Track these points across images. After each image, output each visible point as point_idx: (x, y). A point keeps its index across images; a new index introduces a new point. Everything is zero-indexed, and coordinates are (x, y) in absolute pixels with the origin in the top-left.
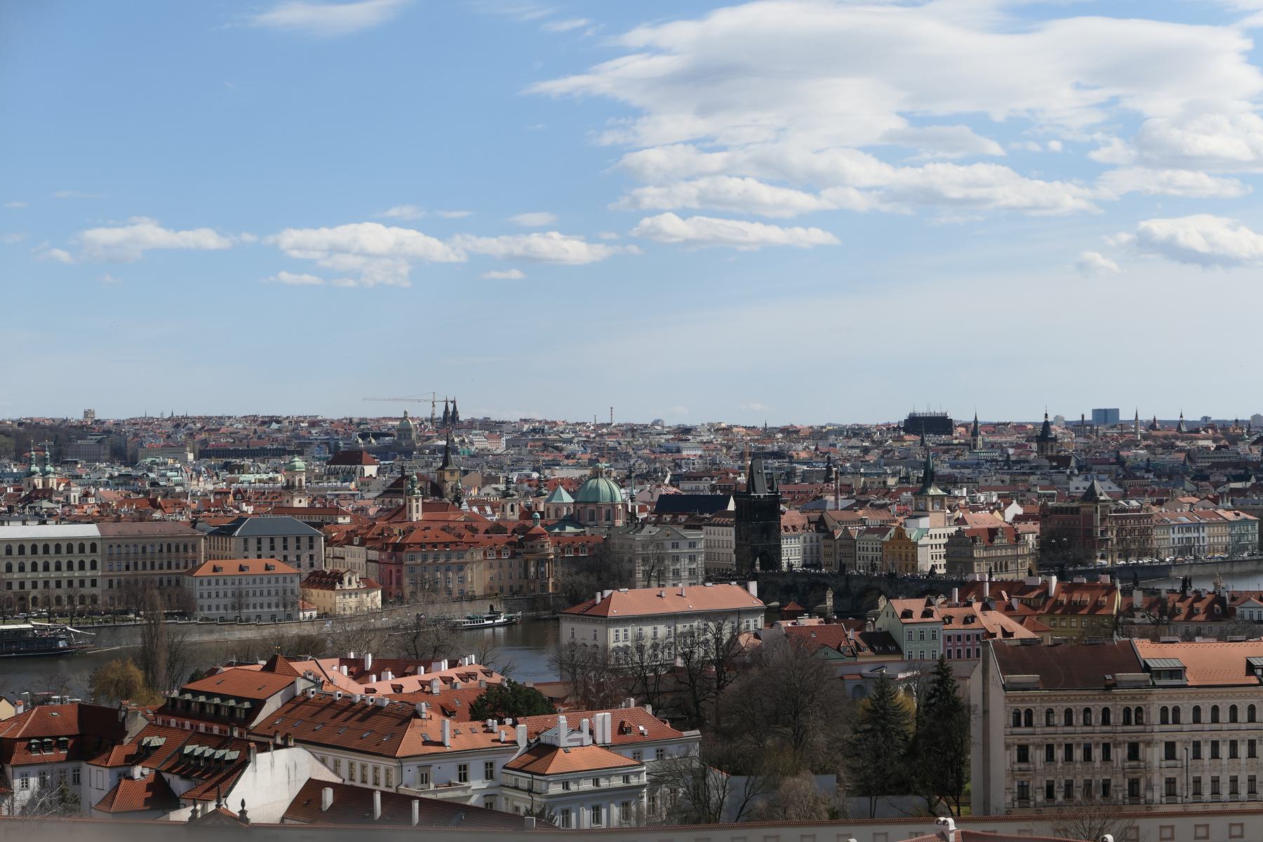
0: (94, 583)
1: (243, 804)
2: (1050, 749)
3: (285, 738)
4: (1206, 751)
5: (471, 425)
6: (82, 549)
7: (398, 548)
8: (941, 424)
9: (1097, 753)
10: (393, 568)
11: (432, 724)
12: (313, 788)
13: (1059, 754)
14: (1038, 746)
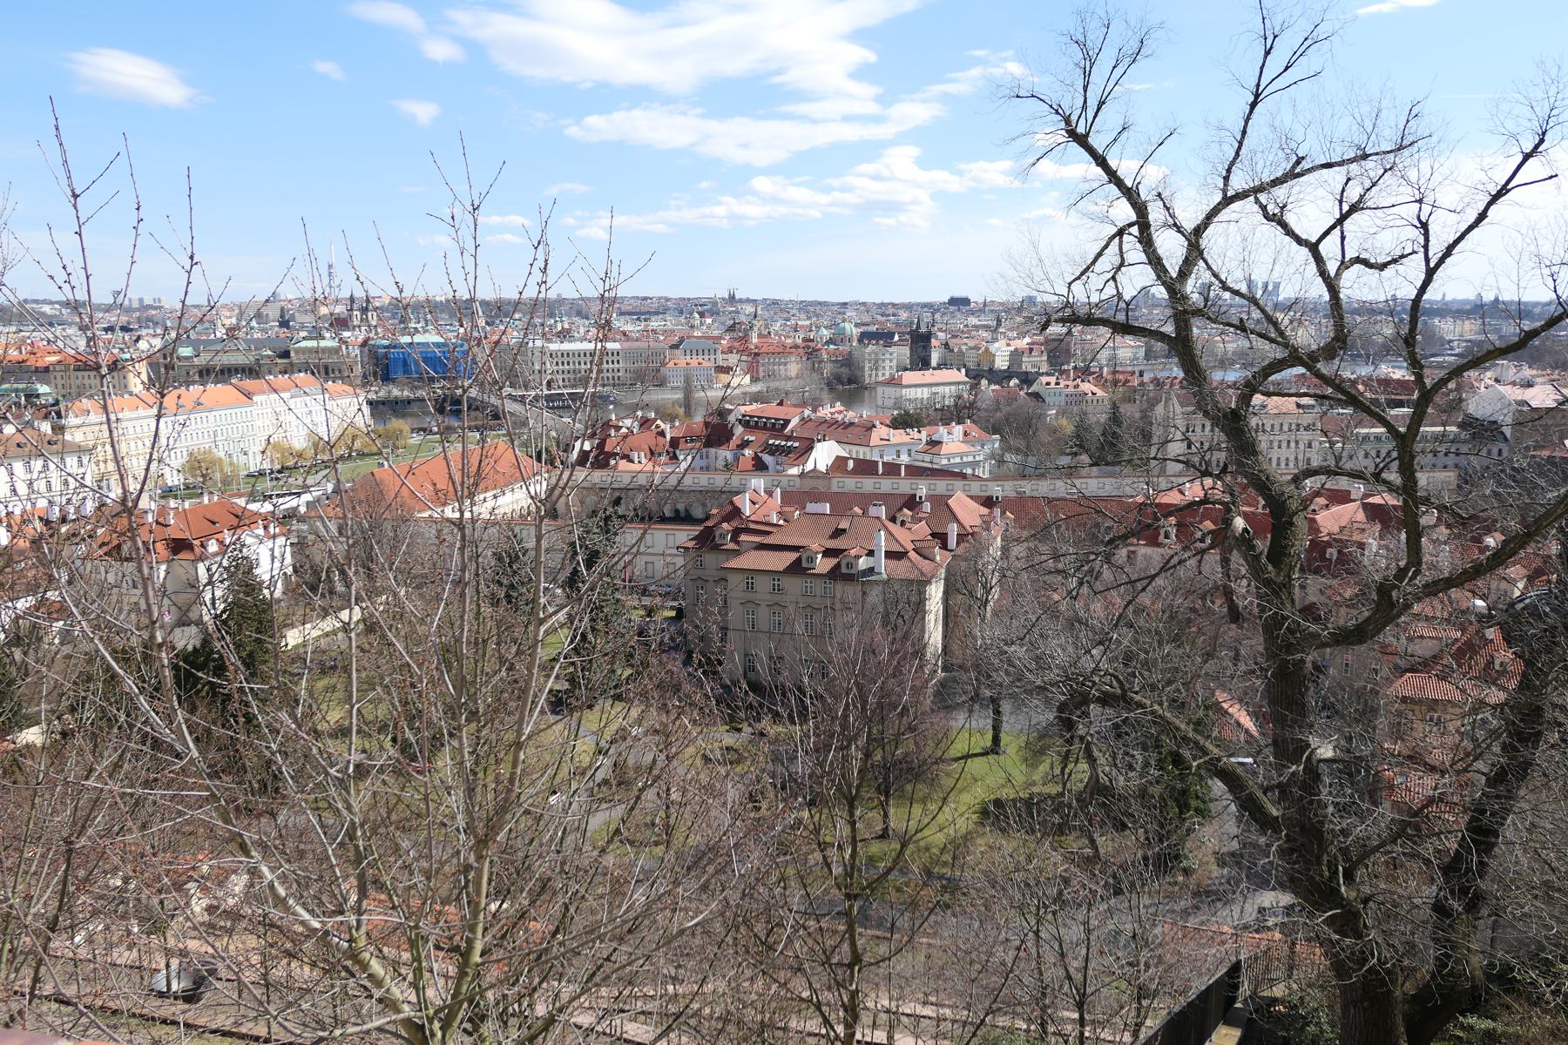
5: (741, 301)
7: (757, 354)
11: (881, 431)
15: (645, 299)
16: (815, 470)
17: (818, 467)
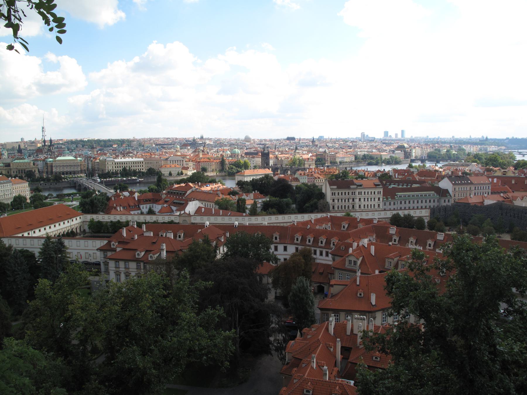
0: (143, 169)
1: (189, 212)
2: (338, 200)
3: (194, 199)
4: (366, 200)
5: (206, 139)
7: (199, 162)
8: (293, 139)
9: (347, 200)
12: (199, 209)
13: (340, 201)
14: (337, 199)
15: (167, 139)
17: (186, 212)
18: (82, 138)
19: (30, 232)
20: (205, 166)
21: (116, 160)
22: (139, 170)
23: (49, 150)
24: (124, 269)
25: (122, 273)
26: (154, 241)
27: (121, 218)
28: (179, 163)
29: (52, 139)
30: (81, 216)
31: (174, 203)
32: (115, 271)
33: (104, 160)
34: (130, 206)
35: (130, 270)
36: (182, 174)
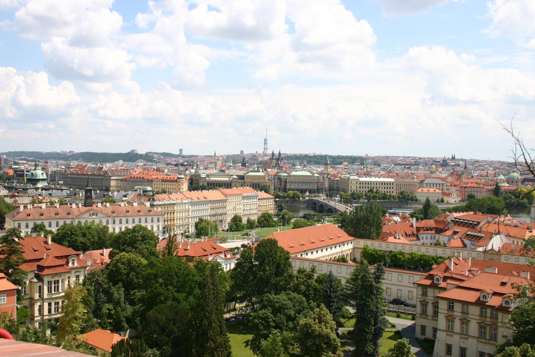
0: (393, 192)
5: (459, 160)
6: (387, 184)
7: (465, 187)
10: (463, 192)
16: (492, 249)
17: (494, 248)
18: (307, 153)
19: (303, 253)
20: (473, 193)
21: (361, 179)
22: (389, 192)
23: (277, 164)
24: (460, 314)
25: (457, 318)
26: (504, 281)
27: (403, 248)
28: (438, 187)
29: (281, 153)
30: (353, 241)
31: (469, 235)
32: (447, 315)
33: (347, 178)
34: (406, 235)
35: (470, 316)
36: (442, 201)
